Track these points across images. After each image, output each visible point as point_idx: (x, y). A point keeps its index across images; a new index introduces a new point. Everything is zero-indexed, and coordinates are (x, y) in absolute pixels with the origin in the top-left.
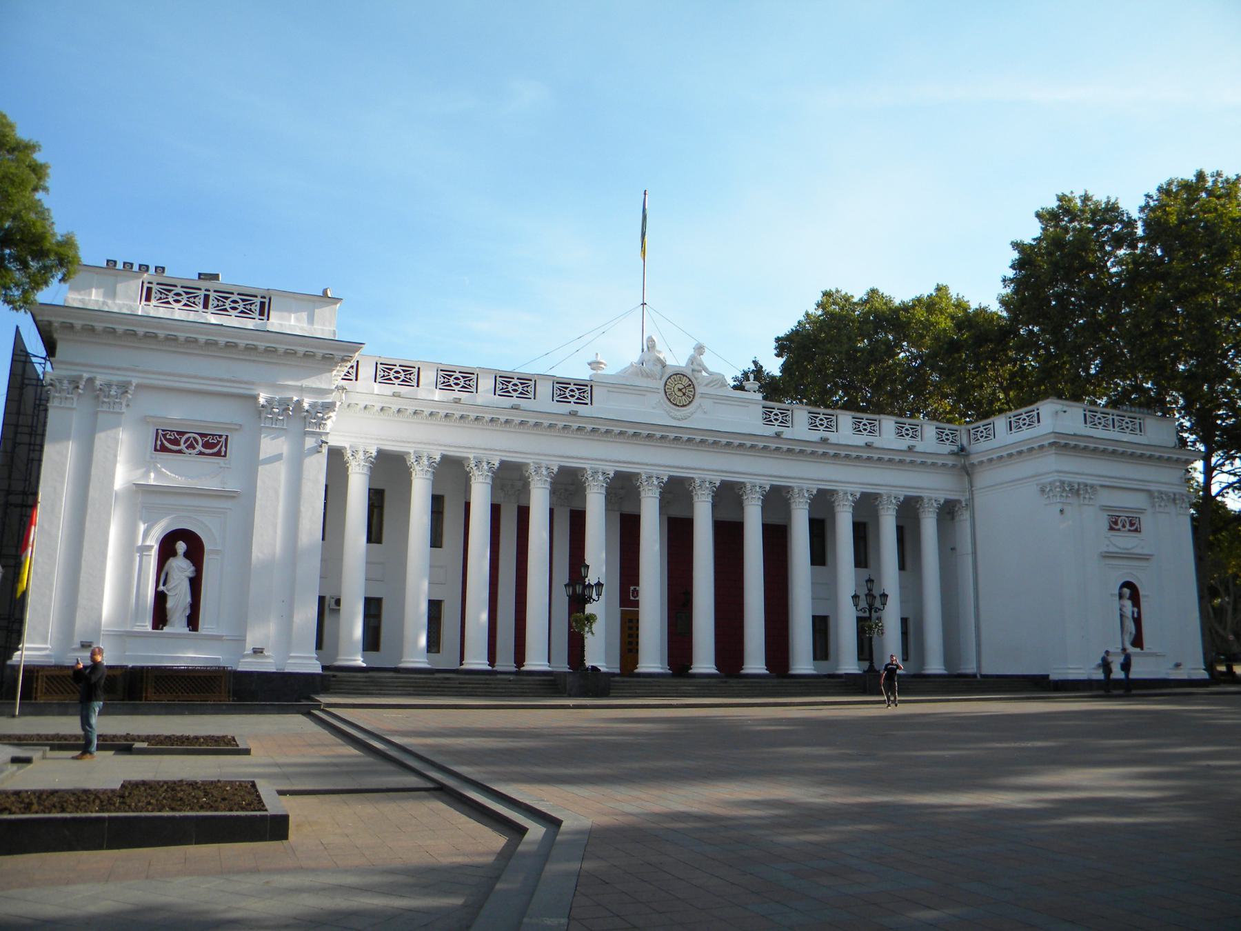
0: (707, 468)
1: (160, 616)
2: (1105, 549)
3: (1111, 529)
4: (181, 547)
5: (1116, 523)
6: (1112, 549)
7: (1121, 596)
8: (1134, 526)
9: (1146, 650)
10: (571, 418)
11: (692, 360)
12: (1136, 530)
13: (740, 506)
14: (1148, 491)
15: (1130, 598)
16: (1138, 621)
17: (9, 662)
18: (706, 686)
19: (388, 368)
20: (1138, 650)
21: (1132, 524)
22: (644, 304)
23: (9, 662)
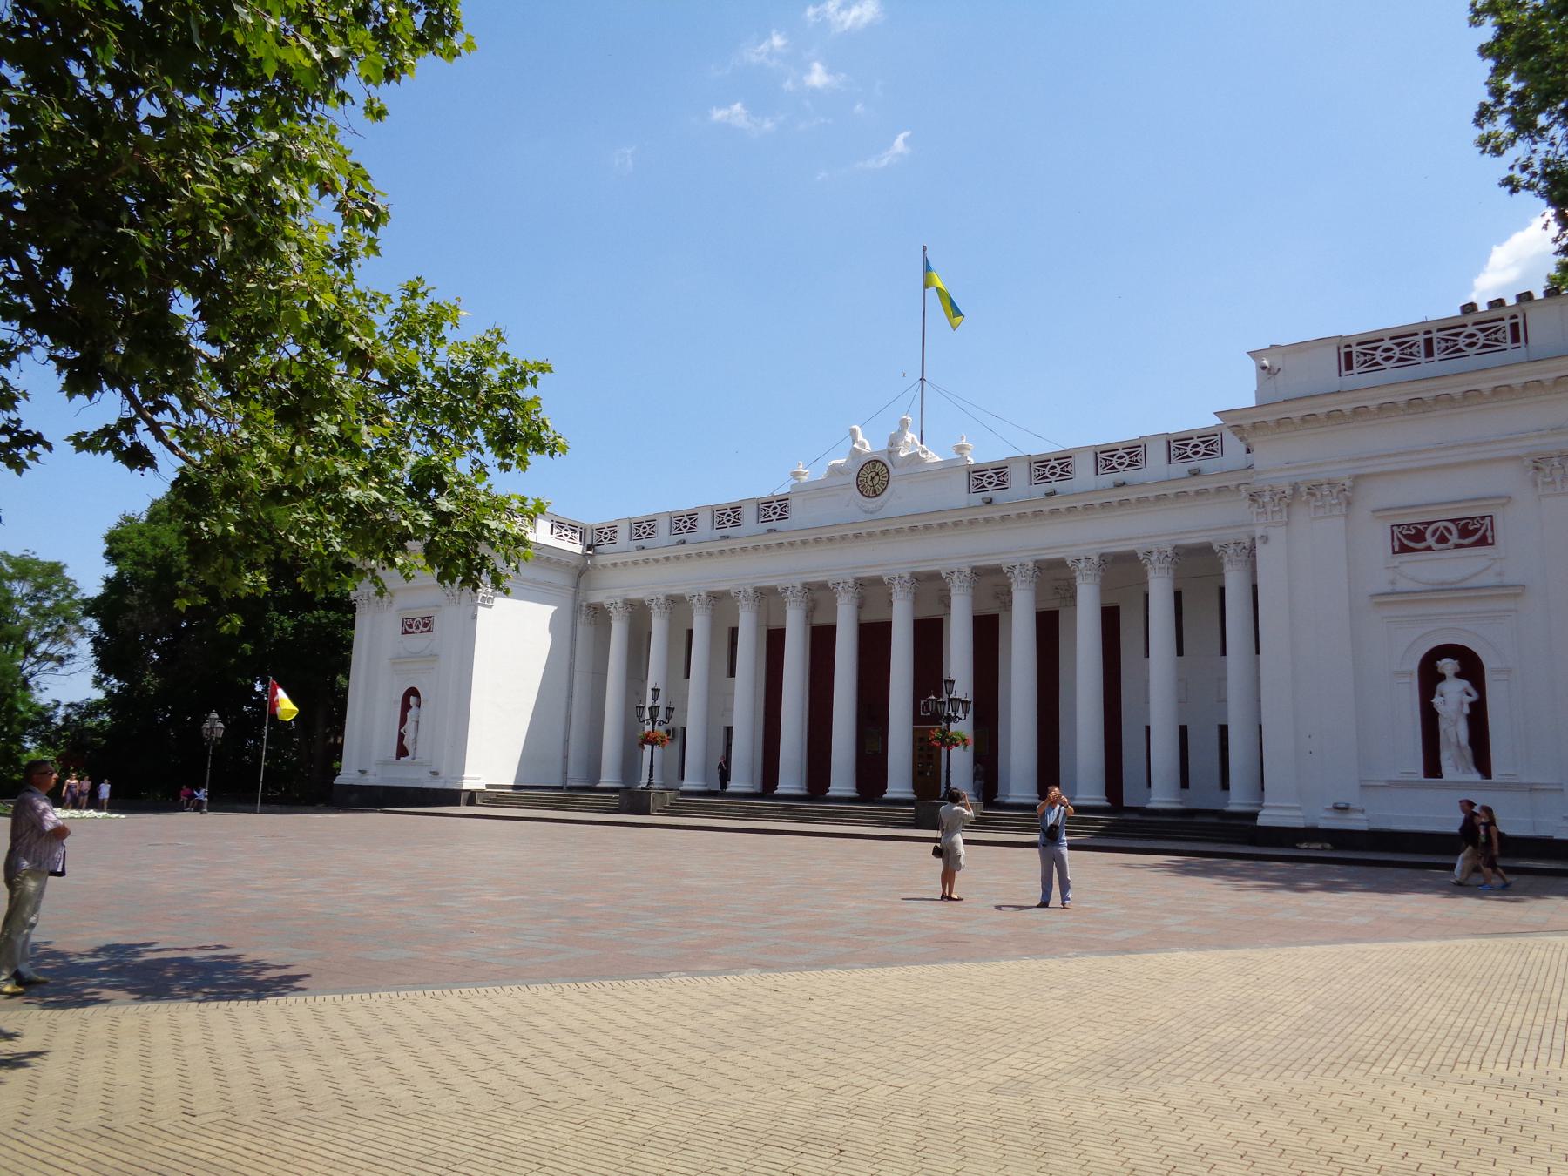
0: (896, 560)
1: (402, 751)
2: (1388, 589)
3: (1404, 549)
4: (413, 700)
5: (1419, 536)
6: (1404, 585)
7: (1429, 677)
8: (1473, 532)
9: (1495, 777)
10: (773, 535)
11: (894, 442)
12: (1482, 542)
13: (945, 600)
14: (1517, 458)
15: (1458, 675)
16: (1477, 718)
17: (338, 781)
18: (840, 811)
19: (638, 524)
20: (1476, 777)
21: (1465, 532)
22: (922, 379)
23: (338, 781)
